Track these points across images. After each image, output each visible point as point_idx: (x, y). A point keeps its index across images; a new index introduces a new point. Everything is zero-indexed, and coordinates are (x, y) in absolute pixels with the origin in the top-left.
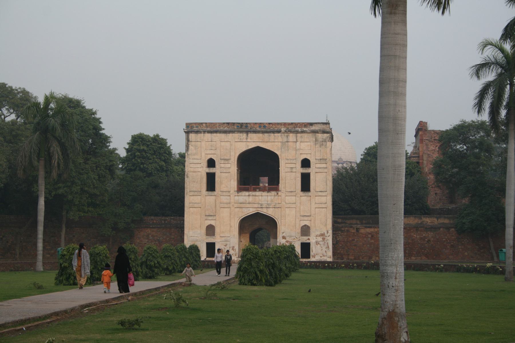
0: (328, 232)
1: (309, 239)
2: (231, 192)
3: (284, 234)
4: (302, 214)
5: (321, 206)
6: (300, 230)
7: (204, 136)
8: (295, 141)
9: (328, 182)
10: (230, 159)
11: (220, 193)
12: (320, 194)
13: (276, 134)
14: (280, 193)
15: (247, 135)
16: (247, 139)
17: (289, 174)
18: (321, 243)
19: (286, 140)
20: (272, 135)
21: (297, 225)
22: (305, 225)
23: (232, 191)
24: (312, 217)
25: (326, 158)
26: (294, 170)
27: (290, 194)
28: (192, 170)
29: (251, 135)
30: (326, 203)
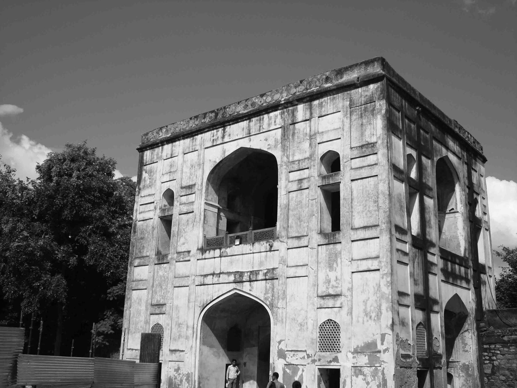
0: (383, 336)
1: (336, 359)
2: (191, 254)
3: (282, 346)
4: (322, 290)
5: (365, 265)
6: (316, 335)
7: (162, 149)
8: (308, 117)
9: (381, 201)
10: (195, 185)
11: (176, 255)
12: (362, 234)
13: (272, 114)
14: (276, 244)
15: (224, 130)
16: (223, 137)
17: (297, 198)
18: (366, 370)
19: (290, 122)
20: (266, 116)
21: (310, 322)
22: (329, 320)
23: (194, 251)
24: (341, 299)
25: (374, 140)
26: (305, 185)
27: (295, 243)
28: (140, 217)
29: (228, 128)
30: (377, 257)
